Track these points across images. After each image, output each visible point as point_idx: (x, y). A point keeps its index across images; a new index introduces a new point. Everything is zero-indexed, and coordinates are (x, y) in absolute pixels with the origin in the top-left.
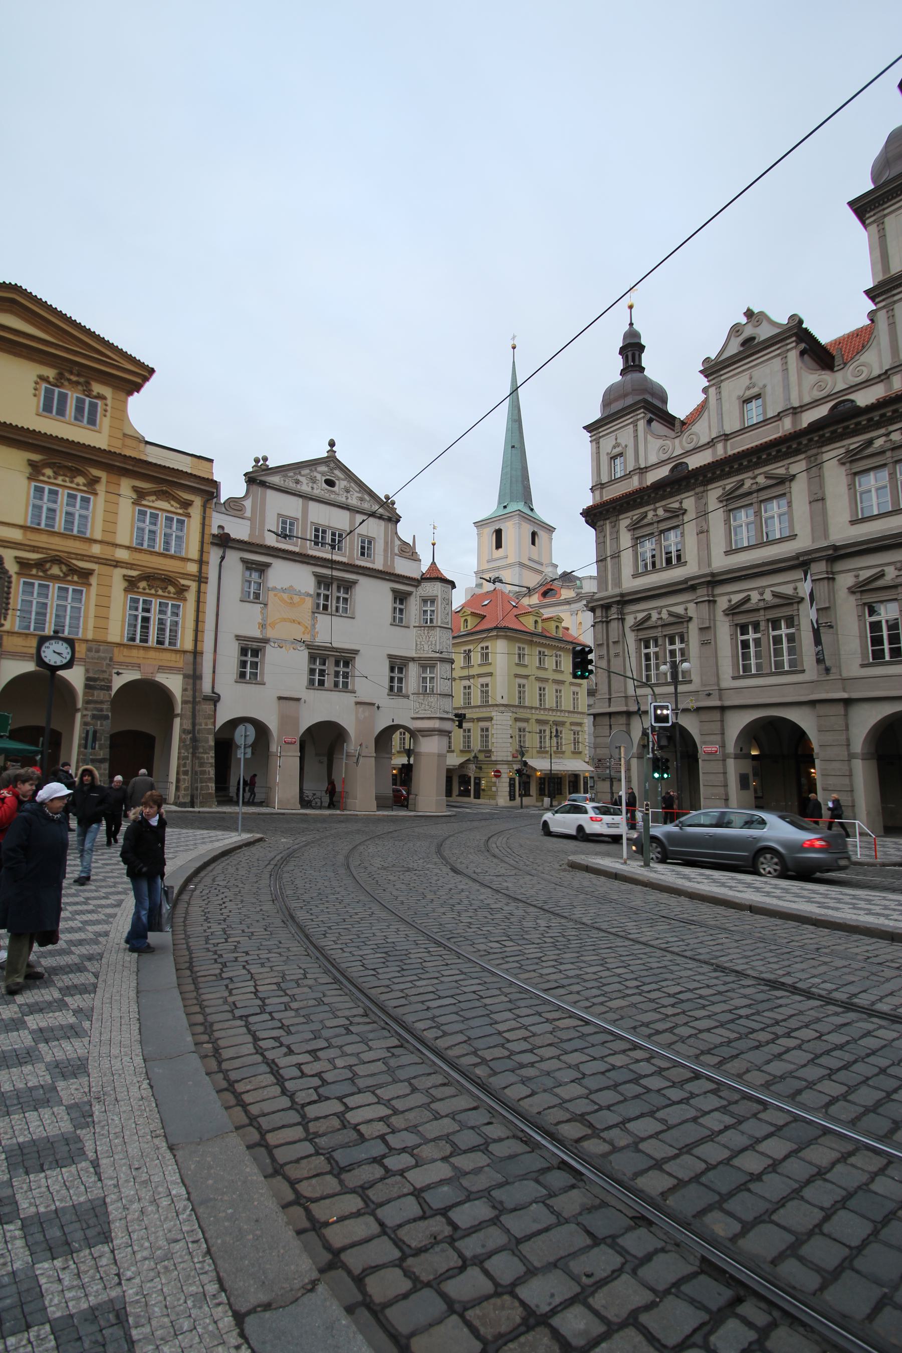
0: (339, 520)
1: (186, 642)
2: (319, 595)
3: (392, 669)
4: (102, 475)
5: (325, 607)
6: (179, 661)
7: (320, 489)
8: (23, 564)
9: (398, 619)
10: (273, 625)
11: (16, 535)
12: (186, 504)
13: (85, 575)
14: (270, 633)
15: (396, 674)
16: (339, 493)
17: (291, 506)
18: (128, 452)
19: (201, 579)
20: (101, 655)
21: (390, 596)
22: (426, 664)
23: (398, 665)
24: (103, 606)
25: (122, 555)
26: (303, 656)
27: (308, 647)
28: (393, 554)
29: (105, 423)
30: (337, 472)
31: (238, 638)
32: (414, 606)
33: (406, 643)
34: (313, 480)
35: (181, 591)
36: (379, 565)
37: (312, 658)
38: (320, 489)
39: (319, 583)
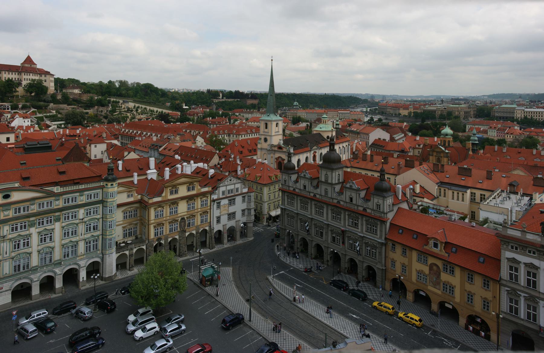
1: (209, 221)
4: (195, 198)
6: (207, 224)
8: (187, 218)
9: (244, 201)
11: (186, 213)
12: (207, 197)
13: (195, 216)
18: (199, 192)
19: (210, 209)
20: (197, 228)
24: (197, 220)
25: (199, 210)
29: (196, 189)
33: (244, 206)
35: (208, 212)
36: (239, 192)
38: (229, 182)
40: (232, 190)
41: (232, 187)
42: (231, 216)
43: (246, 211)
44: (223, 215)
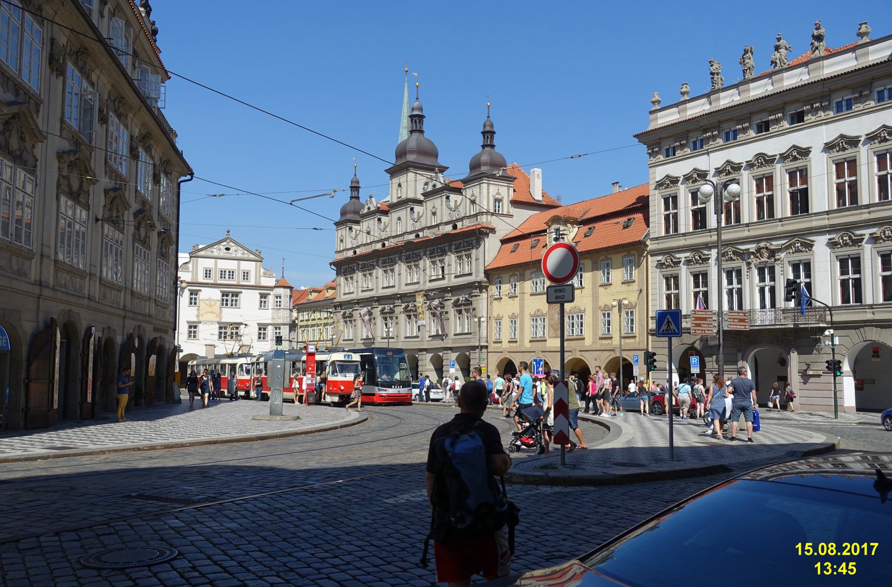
0: (231, 265)
2: (223, 300)
3: (260, 329)
5: (227, 305)
7: (223, 253)
9: (263, 304)
10: (202, 315)
14: (201, 319)
15: (262, 331)
16: (232, 253)
17: (209, 263)
21: (259, 296)
22: (277, 327)
23: (262, 327)
26: (217, 326)
27: (219, 323)
28: (260, 276)
30: (231, 244)
31: (188, 322)
32: (271, 299)
33: (266, 316)
34: (220, 250)
36: (252, 283)
37: (220, 328)
38: (223, 253)
39: (223, 295)
40: (231, 274)
41: (231, 265)
42: (230, 331)
43: (270, 328)
44: (206, 323)
